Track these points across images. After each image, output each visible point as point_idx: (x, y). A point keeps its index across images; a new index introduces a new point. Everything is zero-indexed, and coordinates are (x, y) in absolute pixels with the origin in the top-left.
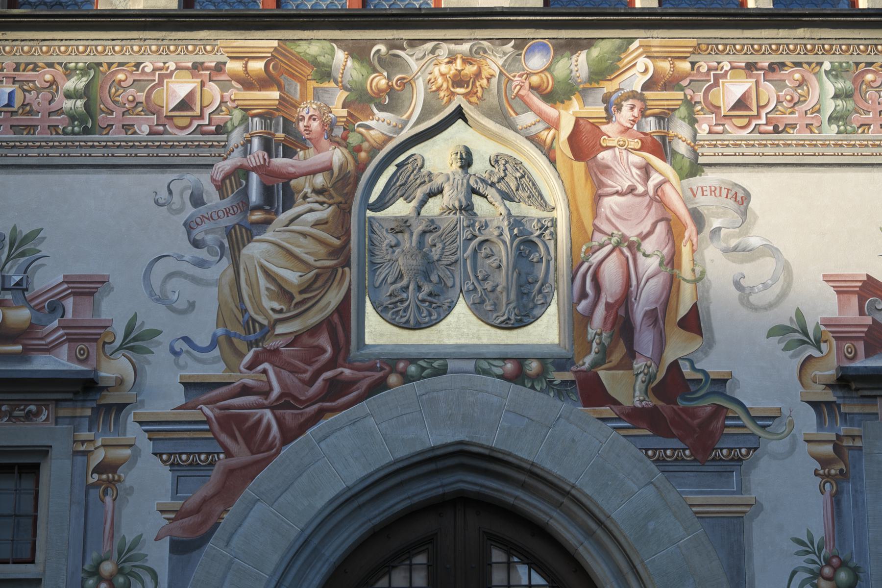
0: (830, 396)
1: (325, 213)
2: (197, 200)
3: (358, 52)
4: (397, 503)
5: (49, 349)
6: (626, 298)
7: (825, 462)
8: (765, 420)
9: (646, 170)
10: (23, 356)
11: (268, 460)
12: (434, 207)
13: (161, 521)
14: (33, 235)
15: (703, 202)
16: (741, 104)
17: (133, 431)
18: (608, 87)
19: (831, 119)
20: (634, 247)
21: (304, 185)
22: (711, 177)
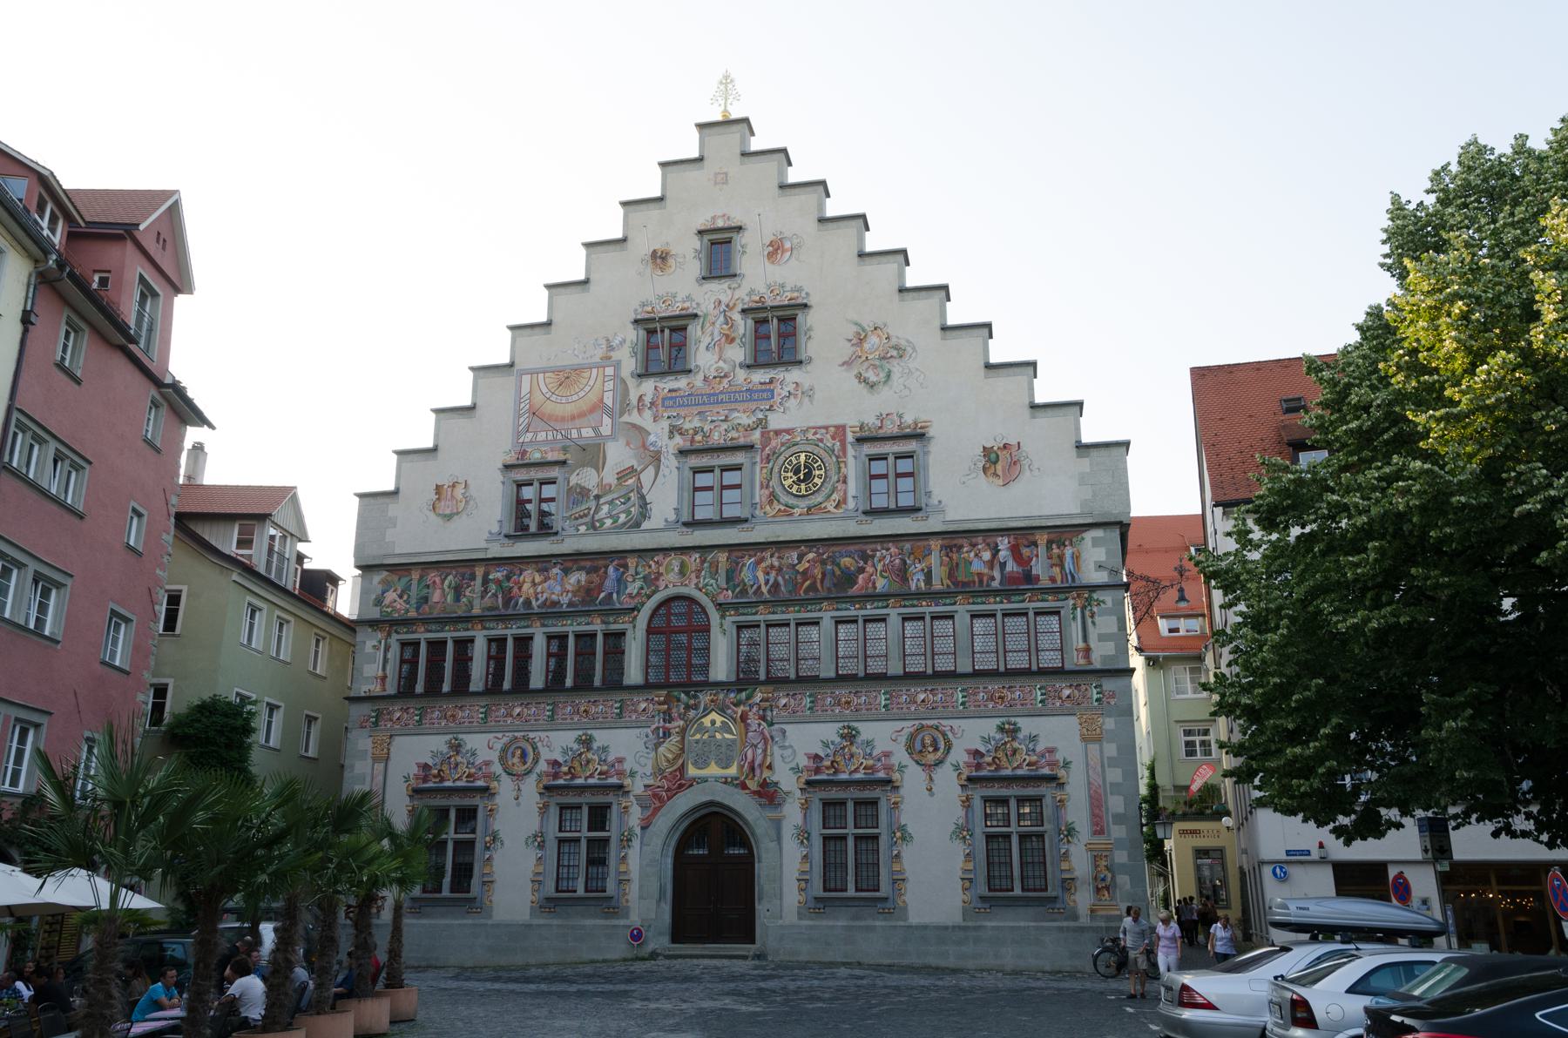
0: (805, 787)
1: (678, 739)
2: (647, 736)
3: (687, 694)
4: (697, 815)
5: (612, 776)
6: (753, 761)
7: (802, 804)
8: (787, 793)
9: (759, 725)
10: (606, 779)
11: (662, 807)
12: (706, 737)
13: (638, 821)
14: (607, 747)
15: (774, 733)
16: (785, 705)
17: (632, 798)
18: (750, 702)
19: (809, 709)
20: (756, 746)
21: (673, 731)
22: (776, 726)
